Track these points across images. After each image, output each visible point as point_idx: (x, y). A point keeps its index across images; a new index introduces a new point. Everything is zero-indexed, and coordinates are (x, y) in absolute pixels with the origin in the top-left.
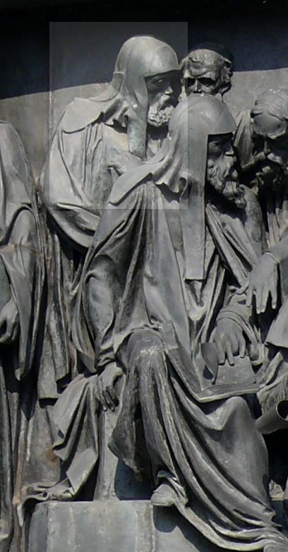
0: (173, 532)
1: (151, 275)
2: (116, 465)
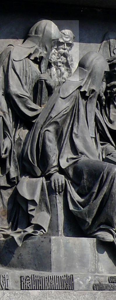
0: (104, 254)
1: (77, 133)
2: (63, 220)
